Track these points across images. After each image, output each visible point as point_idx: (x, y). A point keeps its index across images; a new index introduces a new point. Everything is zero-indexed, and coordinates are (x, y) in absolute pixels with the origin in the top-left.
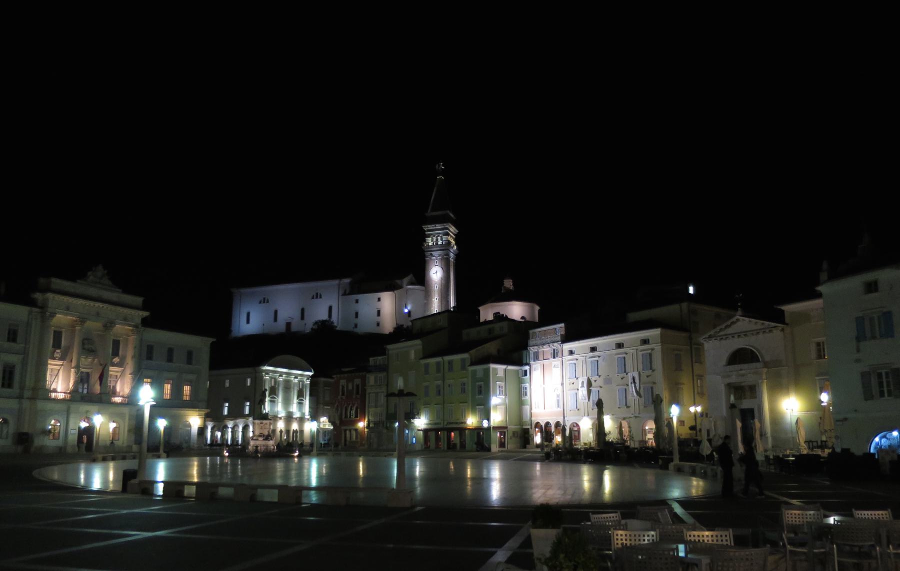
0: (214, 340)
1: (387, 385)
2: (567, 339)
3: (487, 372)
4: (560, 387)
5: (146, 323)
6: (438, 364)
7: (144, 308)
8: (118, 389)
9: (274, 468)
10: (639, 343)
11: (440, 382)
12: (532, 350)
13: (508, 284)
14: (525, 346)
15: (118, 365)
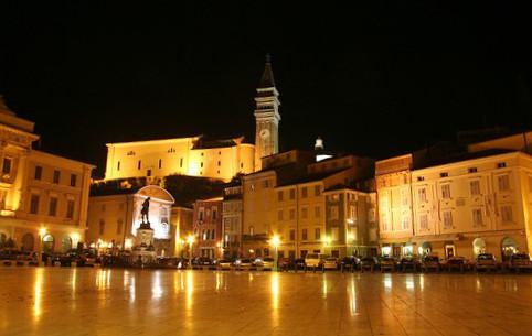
0: (94, 167)
1: (243, 211)
2: (415, 167)
3: (341, 195)
4: (410, 211)
5: (35, 146)
6: (292, 191)
7: (34, 133)
8: (7, 203)
9: (381, 287)
10: (494, 166)
11: (294, 207)
12: (379, 179)
13: (319, 143)
14: (372, 176)
15: (8, 181)
